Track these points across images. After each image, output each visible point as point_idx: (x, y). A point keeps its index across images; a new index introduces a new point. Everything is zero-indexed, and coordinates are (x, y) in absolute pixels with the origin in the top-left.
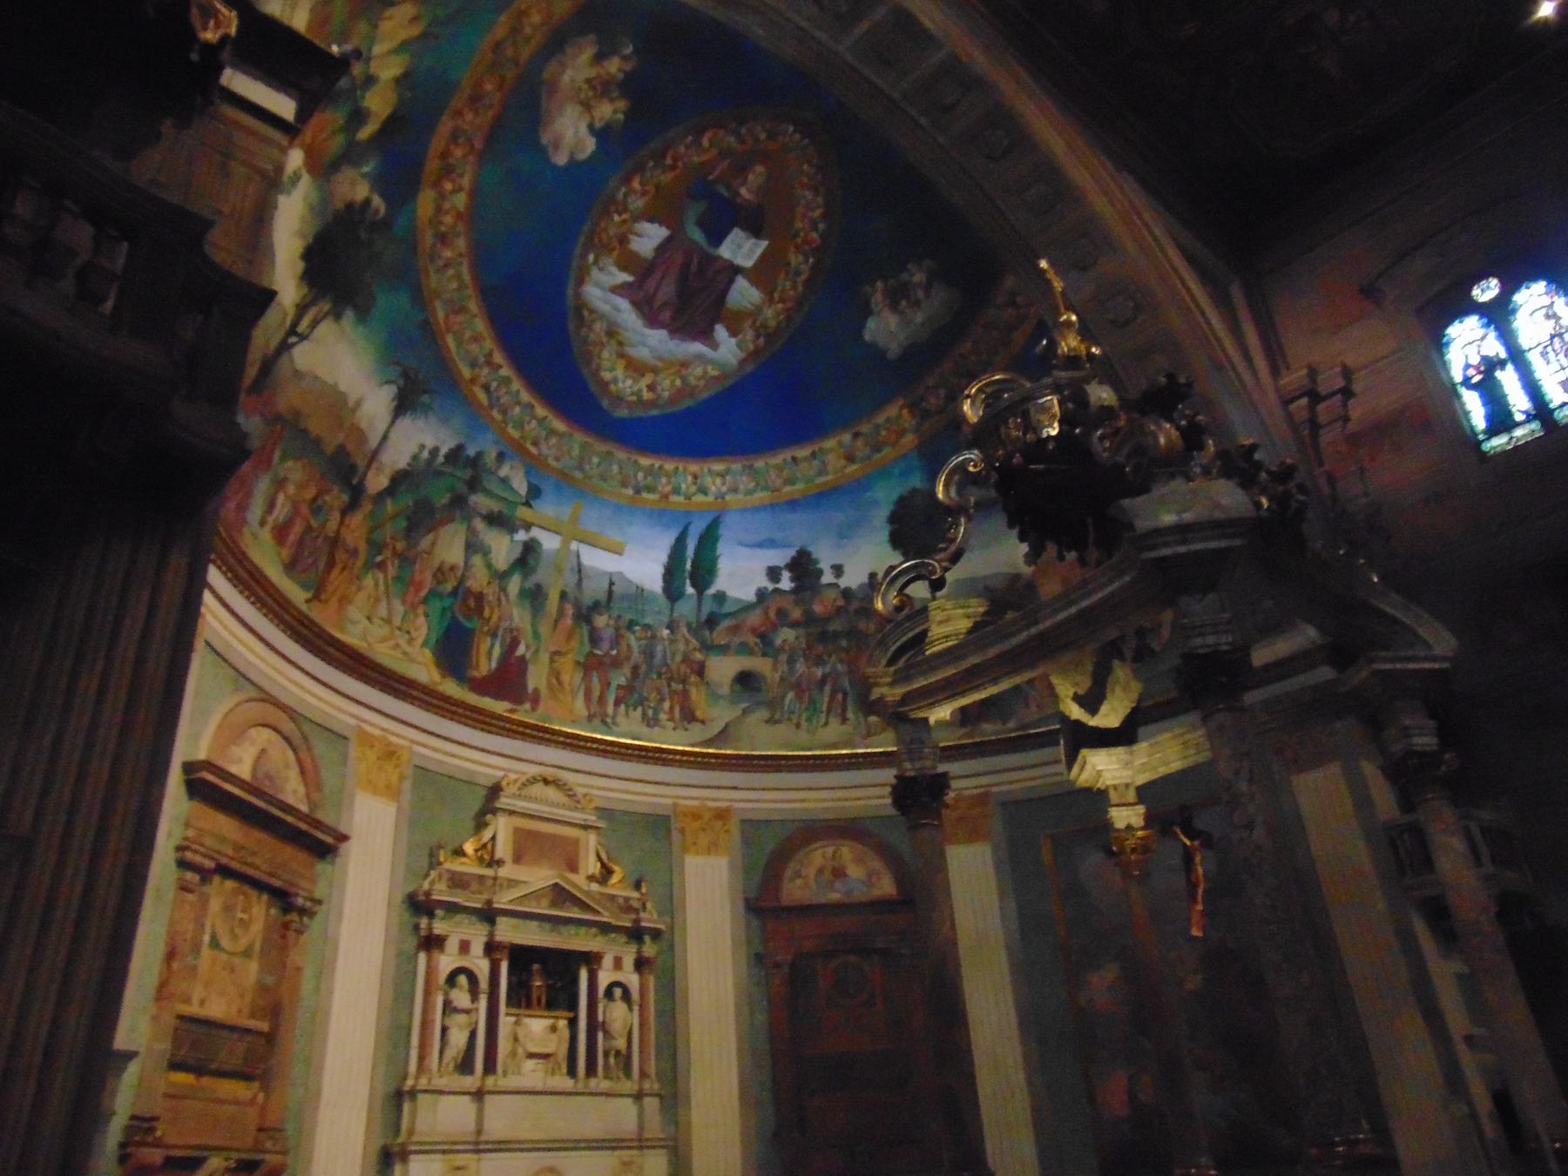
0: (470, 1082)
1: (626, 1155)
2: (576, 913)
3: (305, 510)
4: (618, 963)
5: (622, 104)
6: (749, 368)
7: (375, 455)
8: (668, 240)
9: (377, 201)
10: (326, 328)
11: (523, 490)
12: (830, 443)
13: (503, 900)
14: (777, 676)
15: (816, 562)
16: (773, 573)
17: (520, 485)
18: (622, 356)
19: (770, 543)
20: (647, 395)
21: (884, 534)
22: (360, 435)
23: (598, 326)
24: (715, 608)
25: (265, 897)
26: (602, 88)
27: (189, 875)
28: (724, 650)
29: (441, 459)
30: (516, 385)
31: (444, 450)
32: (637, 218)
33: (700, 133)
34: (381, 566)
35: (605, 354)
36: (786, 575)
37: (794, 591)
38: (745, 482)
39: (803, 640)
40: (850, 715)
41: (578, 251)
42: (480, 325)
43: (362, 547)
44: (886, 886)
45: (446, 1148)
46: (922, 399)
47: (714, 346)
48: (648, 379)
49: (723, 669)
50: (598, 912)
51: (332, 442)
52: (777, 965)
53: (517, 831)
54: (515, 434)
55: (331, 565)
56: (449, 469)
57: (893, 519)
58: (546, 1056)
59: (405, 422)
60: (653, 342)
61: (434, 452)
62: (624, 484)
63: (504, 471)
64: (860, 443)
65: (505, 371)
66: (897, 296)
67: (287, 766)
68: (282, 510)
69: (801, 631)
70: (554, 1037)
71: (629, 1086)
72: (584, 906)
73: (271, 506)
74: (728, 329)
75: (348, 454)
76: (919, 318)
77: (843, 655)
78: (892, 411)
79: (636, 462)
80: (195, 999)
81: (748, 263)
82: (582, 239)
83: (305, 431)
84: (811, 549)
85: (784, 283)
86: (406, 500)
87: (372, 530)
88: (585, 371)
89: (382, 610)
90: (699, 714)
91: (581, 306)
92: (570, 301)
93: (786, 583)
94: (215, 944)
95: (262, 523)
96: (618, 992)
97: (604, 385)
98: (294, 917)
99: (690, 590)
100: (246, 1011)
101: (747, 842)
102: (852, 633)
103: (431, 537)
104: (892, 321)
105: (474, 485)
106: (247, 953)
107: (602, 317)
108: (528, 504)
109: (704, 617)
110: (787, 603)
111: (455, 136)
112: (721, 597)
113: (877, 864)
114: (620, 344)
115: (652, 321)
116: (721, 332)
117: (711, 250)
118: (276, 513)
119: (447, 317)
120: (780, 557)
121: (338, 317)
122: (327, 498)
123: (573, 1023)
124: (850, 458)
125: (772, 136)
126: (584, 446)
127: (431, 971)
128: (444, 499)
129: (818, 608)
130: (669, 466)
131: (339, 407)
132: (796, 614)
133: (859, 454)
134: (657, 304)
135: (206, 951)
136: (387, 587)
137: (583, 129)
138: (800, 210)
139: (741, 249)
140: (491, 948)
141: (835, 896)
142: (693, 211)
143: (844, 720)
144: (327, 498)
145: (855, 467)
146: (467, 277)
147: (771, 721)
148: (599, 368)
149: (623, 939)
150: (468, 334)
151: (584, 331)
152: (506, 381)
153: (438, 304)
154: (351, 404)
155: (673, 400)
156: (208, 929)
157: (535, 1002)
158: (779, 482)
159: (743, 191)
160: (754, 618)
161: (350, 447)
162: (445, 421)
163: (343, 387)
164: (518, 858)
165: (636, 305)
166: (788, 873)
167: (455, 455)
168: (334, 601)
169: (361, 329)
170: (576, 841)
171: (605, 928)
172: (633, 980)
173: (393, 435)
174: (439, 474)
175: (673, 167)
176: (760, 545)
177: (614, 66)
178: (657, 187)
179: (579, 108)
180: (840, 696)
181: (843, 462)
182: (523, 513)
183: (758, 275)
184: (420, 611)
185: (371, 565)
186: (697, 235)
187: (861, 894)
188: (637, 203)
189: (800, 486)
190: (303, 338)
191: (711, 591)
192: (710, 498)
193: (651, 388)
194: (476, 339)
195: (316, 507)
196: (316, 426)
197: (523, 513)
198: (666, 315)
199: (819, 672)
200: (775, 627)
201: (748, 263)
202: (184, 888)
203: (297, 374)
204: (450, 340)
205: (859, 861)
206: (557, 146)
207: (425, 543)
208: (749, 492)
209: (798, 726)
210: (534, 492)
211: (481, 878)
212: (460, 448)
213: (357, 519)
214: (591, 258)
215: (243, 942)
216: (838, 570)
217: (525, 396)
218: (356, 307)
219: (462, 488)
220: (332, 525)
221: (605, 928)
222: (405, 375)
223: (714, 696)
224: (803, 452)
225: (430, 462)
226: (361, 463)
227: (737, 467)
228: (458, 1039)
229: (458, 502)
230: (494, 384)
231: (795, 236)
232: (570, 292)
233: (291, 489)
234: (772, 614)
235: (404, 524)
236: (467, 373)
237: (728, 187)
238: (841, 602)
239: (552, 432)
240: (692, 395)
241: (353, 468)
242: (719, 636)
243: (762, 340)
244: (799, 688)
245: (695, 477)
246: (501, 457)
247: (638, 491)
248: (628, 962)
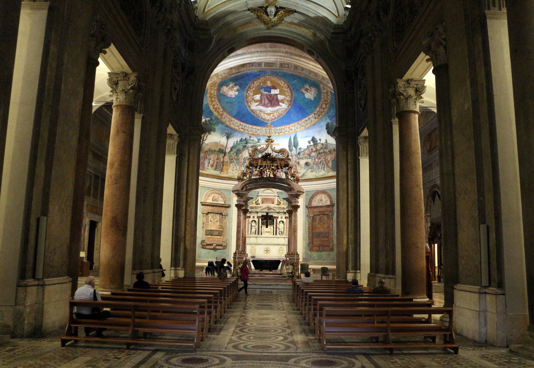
0: (255, 236)
1: (281, 246)
2: (273, 211)
3: (216, 160)
4: (282, 218)
5: (237, 86)
6: (290, 107)
7: (226, 146)
8: (261, 95)
9: (207, 119)
10: (209, 136)
11: (257, 140)
12: (311, 116)
13: (258, 211)
14: (312, 162)
15: (316, 139)
16: (309, 142)
17: (256, 139)
18: (265, 113)
19: (307, 137)
20: (273, 118)
21: (326, 131)
22: (223, 146)
23: (257, 111)
24: (299, 151)
25: (219, 214)
26: (233, 87)
27: (204, 215)
28: (302, 158)
29: (239, 142)
30: (248, 125)
31: (239, 141)
32: (253, 95)
33: (253, 83)
34: (233, 162)
35: (262, 114)
36: (311, 142)
37: (313, 145)
38: (299, 126)
39: (316, 155)
40: (325, 169)
41: (246, 104)
42: (236, 121)
43: (228, 160)
44: (328, 203)
45: (251, 244)
46: (322, 106)
47: (281, 106)
48: (272, 115)
49: (303, 162)
50: (276, 210)
51: (217, 149)
52: (310, 217)
53: (262, 198)
54: (251, 133)
55: (223, 165)
56: (241, 143)
57: (327, 128)
58: (269, 232)
59: (230, 140)
60: (270, 110)
61: (237, 141)
62: (276, 133)
63: (252, 139)
64: (316, 115)
65: (244, 124)
66: (307, 90)
67: (219, 197)
68: (211, 162)
69: (316, 153)
70: (270, 229)
71: (284, 236)
72: (274, 210)
73: (209, 163)
74: (282, 102)
75: (221, 149)
76: (313, 93)
77: (323, 157)
78: (318, 109)
79: (276, 129)
81: (278, 93)
82: (246, 102)
83: (212, 150)
84: (314, 136)
85: (287, 94)
86: (234, 150)
87: (230, 157)
88: (259, 118)
89: (235, 168)
90: (299, 172)
91: (252, 111)
92: (250, 111)
93: (312, 144)
94: (211, 221)
95: (208, 166)
96: (281, 222)
97: (264, 119)
98: (224, 216)
99: (294, 148)
100: (218, 228)
101: (307, 195)
102: (324, 152)
103: (241, 154)
104: (309, 94)
105: (246, 143)
106: (217, 221)
107: (258, 110)
108: (259, 142)
109: (298, 153)
110: (312, 147)
111: (214, 105)
112: (300, 149)
113: (328, 199)
114: (264, 112)
115: (267, 107)
116: (281, 104)
117: (270, 94)
118: (210, 163)
119: (229, 123)
120: (310, 139)
121: (210, 134)
122: (220, 157)
123: (274, 227)
124: (316, 118)
125: (265, 78)
126: (265, 129)
127: (249, 221)
128: (242, 147)
129: (318, 148)
130: (283, 127)
131: (216, 144)
132: (314, 149)
133: (317, 117)
134: (266, 104)
136: (235, 165)
137: (234, 92)
138: (280, 83)
139: (273, 92)
140: (258, 217)
141: (320, 205)
142: (262, 91)
143: (324, 170)
144: (220, 157)
145: (317, 120)
146: (229, 117)
147: (312, 171)
148: (262, 117)
149: (283, 214)
150: (234, 123)
151: (255, 113)
152: (246, 126)
153: (227, 122)
154: (218, 142)
155: (278, 117)
156: (209, 220)
158: (305, 125)
159: (268, 85)
160: (307, 152)
161: (221, 148)
162: (237, 136)
163: (216, 141)
164: (262, 203)
165: (262, 106)
166: (313, 200)
167: (241, 140)
168: (225, 171)
169: (215, 133)
170: (274, 199)
171: (278, 213)
172: (284, 220)
173: (228, 142)
174: (239, 144)
175: (253, 88)
176: (305, 137)
177: (231, 85)
178: (253, 91)
179: (231, 91)
180: (323, 165)
181: (314, 119)
182: (258, 144)
183: (281, 93)
184: (242, 166)
185: (231, 162)
186: (267, 93)
187: (325, 204)
188: (252, 94)
189: (309, 125)
190: (205, 140)
191: (298, 148)
192: (293, 131)
193: (273, 116)
194: (237, 123)
195: (218, 159)
196: (213, 149)
197: (258, 144)
198: (269, 105)
199: (320, 161)
200: (311, 153)
201: (278, 93)
203: (207, 144)
204: (232, 125)
205: (325, 198)
206: (232, 96)
207: (240, 155)
208: (300, 128)
209: (316, 172)
210: (259, 140)
211: (256, 207)
212: (241, 139)
213: (226, 157)
214: (249, 104)
215: (216, 220)
216: (320, 140)
217: (250, 126)
218: (212, 131)
219: (245, 144)
220: (222, 160)
221: (278, 213)
222: (226, 134)
223: (302, 168)
224: (307, 119)
225: (237, 143)
226: (224, 149)
227: (296, 124)
228: (253, 230)
229: (245, 147)
230: (243, 128)
231: (283, 87)
232: (249, 110)
233: (212, 159)
234: (310, 150)
235: (235, 154)
236: (237, 128)
237: (265, 85)
238: (322, 146)
239: (258, 129)
240: (282, 115)
241: (223, 150)
242: (301, 156)
243: (289, 102)
244: (316, 164)
245: (289, 128)
246: (250, 137)
247: (279, 133)
248: (284, 217)
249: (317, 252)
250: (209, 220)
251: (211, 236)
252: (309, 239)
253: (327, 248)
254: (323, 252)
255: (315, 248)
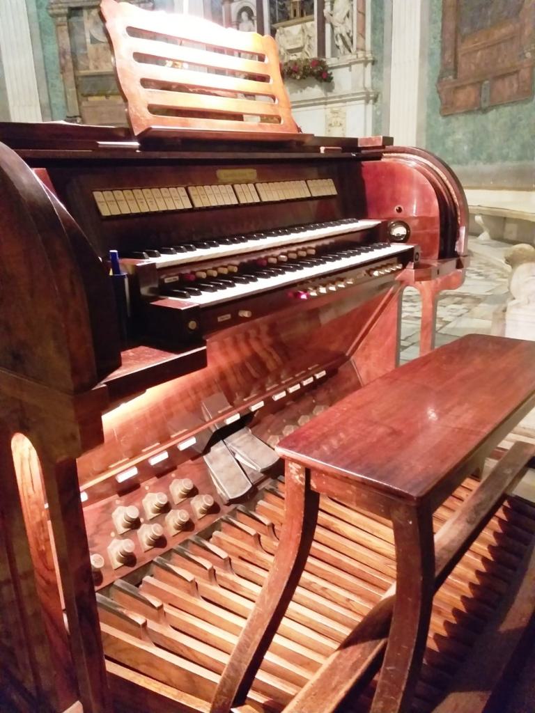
27: (59, 19)
80: (91, 67)
135: (90, 46)
156: (88, 36)
157: (292, 15)
202: (58, 25)
249: (469, 117)
250: (88, 36)
251: (103, 98)
252: (443, 50)
253: (507, 81)
254: (492, 115)
255: (462, 96)
